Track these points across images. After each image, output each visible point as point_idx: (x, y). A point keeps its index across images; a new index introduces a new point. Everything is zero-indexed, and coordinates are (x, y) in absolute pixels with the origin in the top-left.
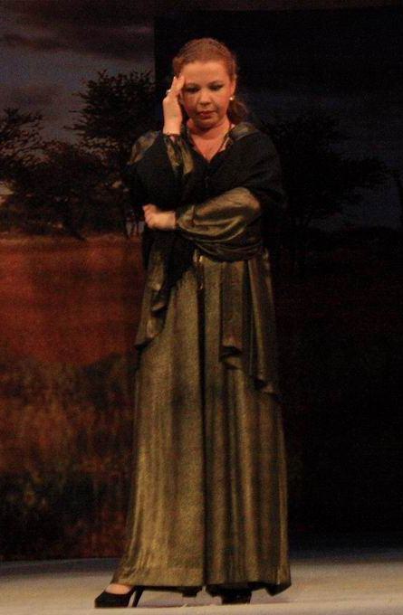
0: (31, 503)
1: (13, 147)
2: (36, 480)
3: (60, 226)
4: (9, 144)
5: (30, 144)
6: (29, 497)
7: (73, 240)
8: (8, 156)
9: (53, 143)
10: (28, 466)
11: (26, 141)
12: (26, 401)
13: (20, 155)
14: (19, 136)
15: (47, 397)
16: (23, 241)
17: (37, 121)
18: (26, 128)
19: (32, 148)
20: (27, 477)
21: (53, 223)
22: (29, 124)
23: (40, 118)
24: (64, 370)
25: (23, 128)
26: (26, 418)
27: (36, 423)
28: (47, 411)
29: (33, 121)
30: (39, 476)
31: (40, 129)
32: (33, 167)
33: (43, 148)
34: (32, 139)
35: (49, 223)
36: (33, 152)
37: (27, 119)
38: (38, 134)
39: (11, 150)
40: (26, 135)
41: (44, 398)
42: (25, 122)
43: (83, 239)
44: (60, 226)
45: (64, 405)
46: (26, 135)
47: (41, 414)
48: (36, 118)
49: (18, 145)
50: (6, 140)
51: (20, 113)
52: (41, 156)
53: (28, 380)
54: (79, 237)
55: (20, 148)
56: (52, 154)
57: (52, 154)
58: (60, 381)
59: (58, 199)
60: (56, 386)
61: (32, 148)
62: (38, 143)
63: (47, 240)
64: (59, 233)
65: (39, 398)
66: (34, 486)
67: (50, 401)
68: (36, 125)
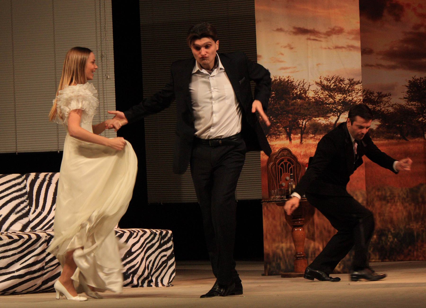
0: (391, 240)
1: (352, 96)
2: (393, 232)
3: (399, 136)
4: (350, 95)
5: (387, 105)
6: (390, 238)
7: (404, 141)
8: (350, 100)
9: (395, 104)
10: (389, 226)
11: (385, 104)
12: (388, 202)
13: (355, 99)
14: (354, 91)
15: (396, 200)
16: (386, 142)
17: (389, 96)
18: (385, 99)
19: (387, 107)
20: (389, 231)
21: (396, 135)
22: (387, 97)
23: (390, 95)
24: (402, 190)
25: (356, 87)
26: (388, 209)
27: (392, 210)
28: (396, 205)
29: (388, 96)
30: (394, 230)
31: (390, 99)
32: (388, 113)
33: (392, 106)
34: (387, 103)
35: (395, 135)
36: (388, 108)
37: (386, 96)
38: (390, 101)
39: (351, 97)
40: (357, 90)
41: (394, 201)
42: (357, 84)
43: (408, 141)
44: (399, 136)
45: (402, 203)
46: (357, 90)
47: (394, 207)
48: (388, 95)
49: (382, 106)
50: (348, 93)
51: (355, 80)
52: (391, 110)
53: (388, 194)
54: (406, 140)
55: (383, 107)
56: (395, 109)
57: (395, 109)
58: (401, 194)
59: (398, 126)
60: (399, 196)
61: (387, 107)
62: (390, 105)
63: (394, 141)
64: (400, 138)
65: (393, 201)
66: (392, 234)
67: (397, 202)
68: (389, 98)
